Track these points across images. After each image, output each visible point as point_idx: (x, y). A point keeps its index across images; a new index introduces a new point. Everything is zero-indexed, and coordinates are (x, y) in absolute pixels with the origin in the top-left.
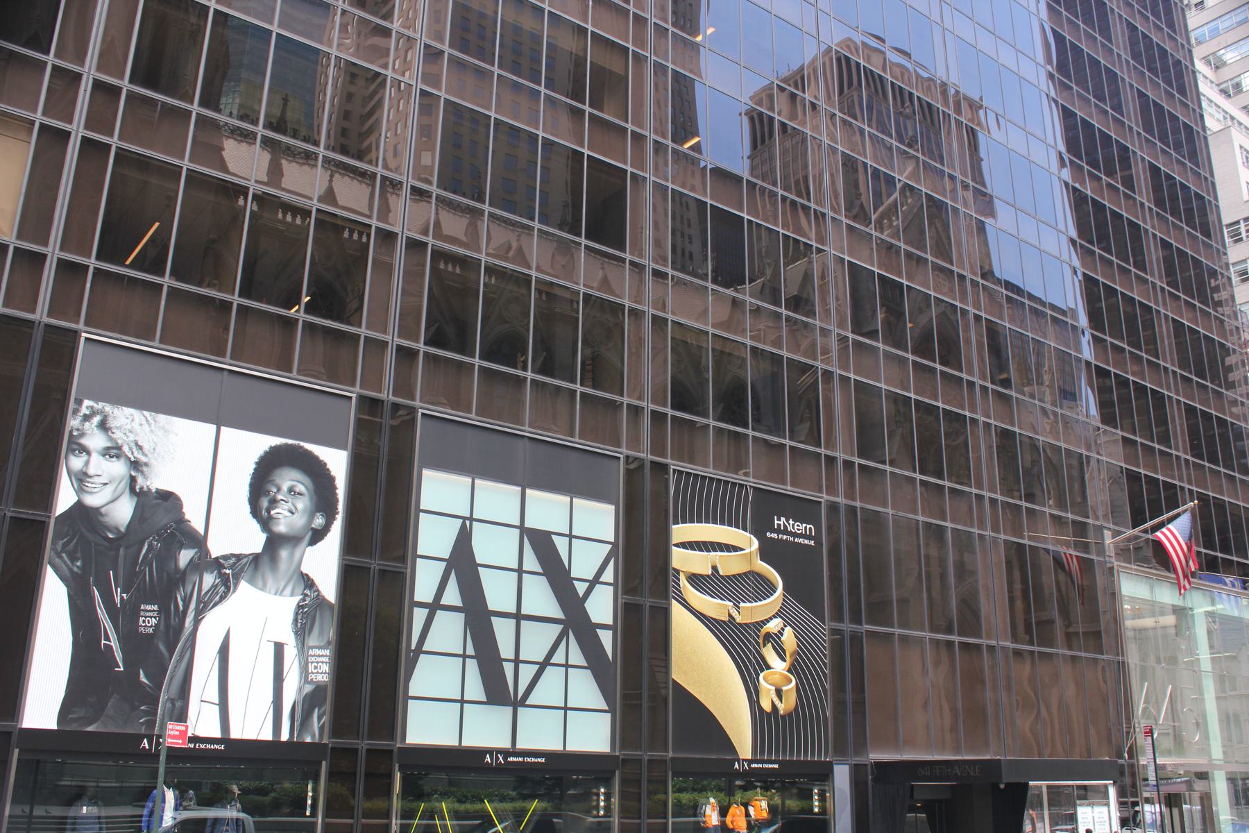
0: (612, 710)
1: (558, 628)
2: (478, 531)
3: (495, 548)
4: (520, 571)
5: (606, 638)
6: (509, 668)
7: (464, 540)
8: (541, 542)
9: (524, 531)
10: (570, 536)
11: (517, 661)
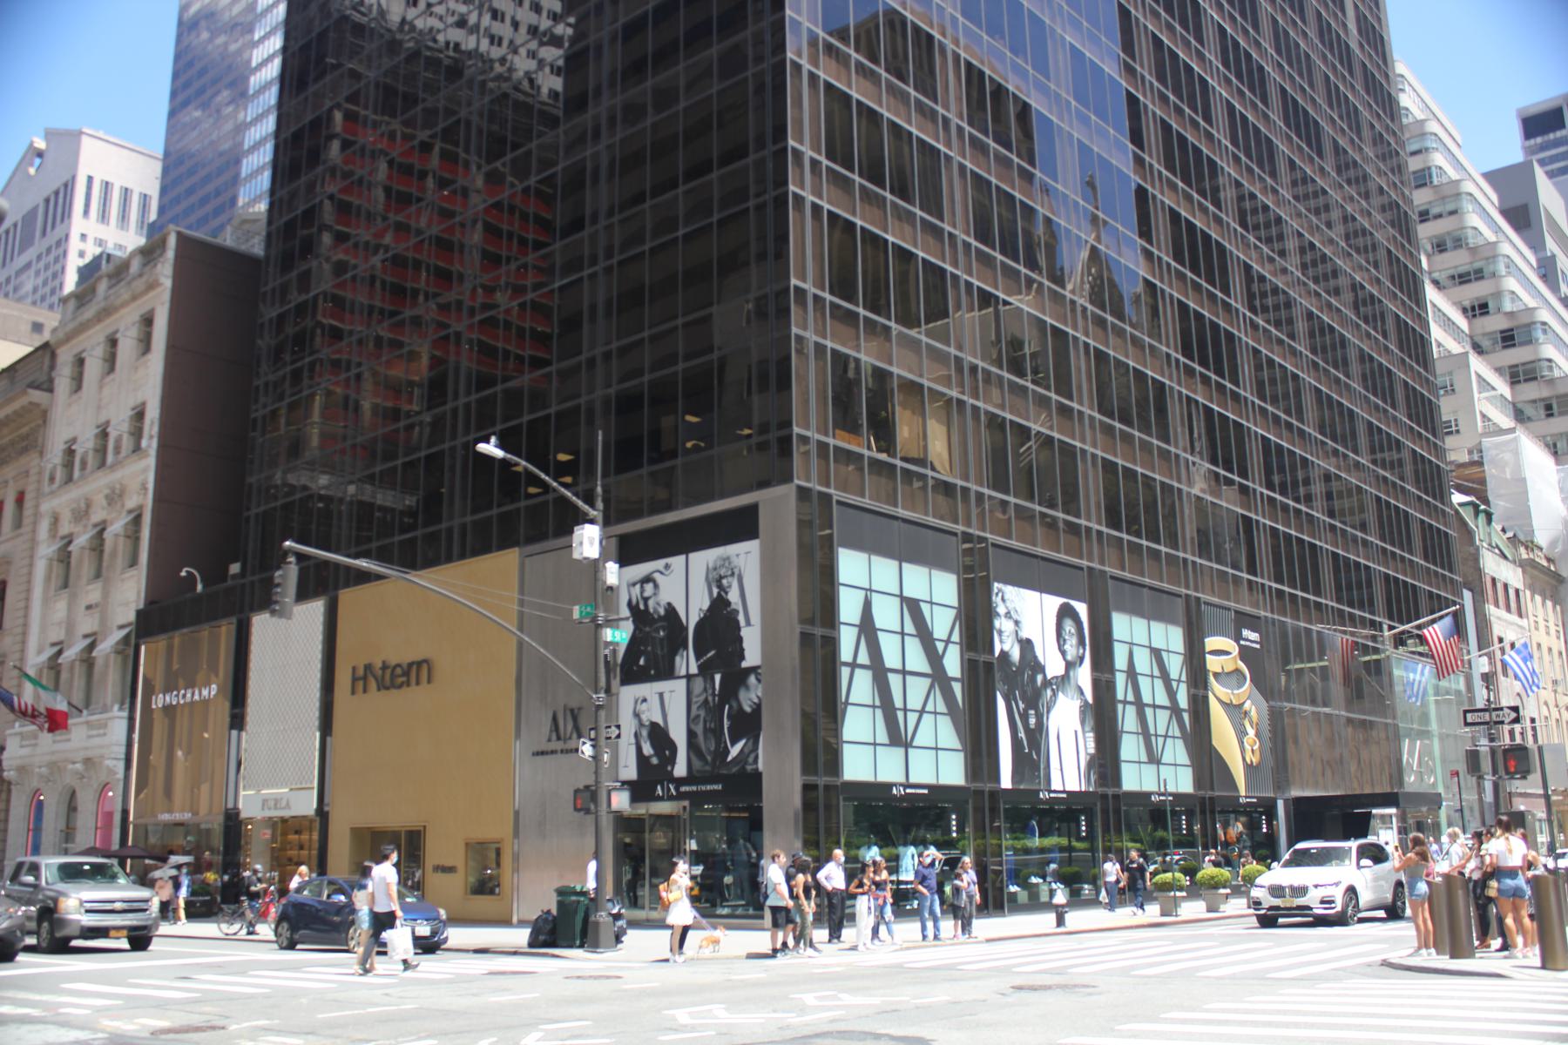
0: (964, 750)
1: (928, 681)
2: (875, 598)
3: (887, 615)
4: (902, 634)
5: (957, 688)
6: (900, 715)
7: (867, 605)
8: (912, 607)
9: (901, 596)
10: (931, 603)
11: (905, 710)
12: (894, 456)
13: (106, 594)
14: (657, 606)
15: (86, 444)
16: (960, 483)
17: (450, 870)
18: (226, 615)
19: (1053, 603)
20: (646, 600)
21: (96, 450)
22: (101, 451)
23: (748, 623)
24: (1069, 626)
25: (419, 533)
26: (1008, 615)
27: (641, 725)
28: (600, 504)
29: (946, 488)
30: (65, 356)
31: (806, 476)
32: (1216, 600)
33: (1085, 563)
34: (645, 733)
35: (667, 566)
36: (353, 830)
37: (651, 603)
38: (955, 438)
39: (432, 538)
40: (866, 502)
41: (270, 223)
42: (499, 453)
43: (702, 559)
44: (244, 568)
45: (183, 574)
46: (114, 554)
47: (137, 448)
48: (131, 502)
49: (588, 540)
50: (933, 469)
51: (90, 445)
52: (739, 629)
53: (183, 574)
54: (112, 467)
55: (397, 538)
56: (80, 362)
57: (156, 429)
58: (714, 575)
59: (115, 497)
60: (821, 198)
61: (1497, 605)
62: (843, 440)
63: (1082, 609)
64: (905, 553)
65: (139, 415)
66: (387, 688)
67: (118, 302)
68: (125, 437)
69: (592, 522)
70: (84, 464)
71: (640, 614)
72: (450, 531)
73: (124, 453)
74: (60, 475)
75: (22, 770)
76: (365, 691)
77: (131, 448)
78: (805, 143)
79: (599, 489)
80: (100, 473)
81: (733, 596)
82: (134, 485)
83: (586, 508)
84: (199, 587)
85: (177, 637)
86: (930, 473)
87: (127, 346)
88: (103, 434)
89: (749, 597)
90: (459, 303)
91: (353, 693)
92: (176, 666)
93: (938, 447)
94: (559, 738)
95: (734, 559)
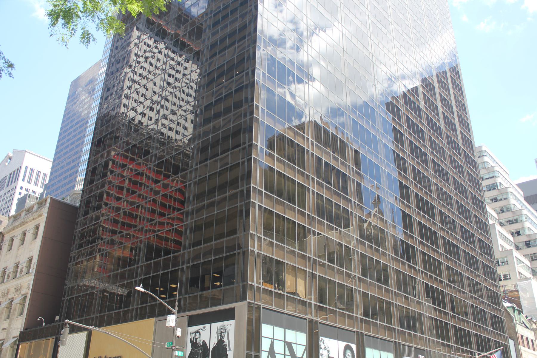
3: (279, 348)
4: (285, 355)
7: (272, 345)
8: (289, 345)
9: (285, 341)
10: (296, 344)
12: (284, 292)
13: (10, 325)
14: (200, 342)
15: (11, 269)
16: (308, 301)
18: (51, 336)
19: (343, 344)
20: (196, 339)
21: (14, 272)
22: (15, 272)
23: (230, 350)
24: (348, 352)
25: (122, 310)
26: (325, 348)
28: (177, 308)
29: (303, 303)
30: (7, 238)
31: (253, 298)
32: (407, 344)
33: (355, 330)
35: (204, 327)
37: (198, 340)
38: (307, 285)
39: (126, 312)
40: (274, 308)
41: (82, 197)
42: (143, 290)
43: (216, 326)
44: (60, 318)
46: (15, 309)
47: (28, 273)
48: (23, 292)
49: (171, 320)
50: (299, 296)
51: (12, 270)
52: (227, 351)
55: (114, 312)
56: (12, 240)
57: (35, 266)
58: (219, 331)
59: (18, 289)
60: (262, 203)
61: (524, 346)
62: (266, 286)
63: (354, 346)
64: (286, 326)
65: (30, 260)
67: (28, 220)
68: (24, 268)
69: (173, 314)
70: (8, 276)
71: (194, 344)
72: (133, 309)
73: (23, 274)
77: (26, 272)
78: (257, 184)
79: (177, 303)
80: (14, 280)
81: (225, 340)
82: (25, 285)
83: (172, 309)
84: (44, 324)
85: (34, 343)
86: (297, 298)
87: (29, 236)
88: (17, 266)
89: (230, 340)
90: (142, 228)
92: (31, 354)
93: (301, 288)
95: (226, 326)
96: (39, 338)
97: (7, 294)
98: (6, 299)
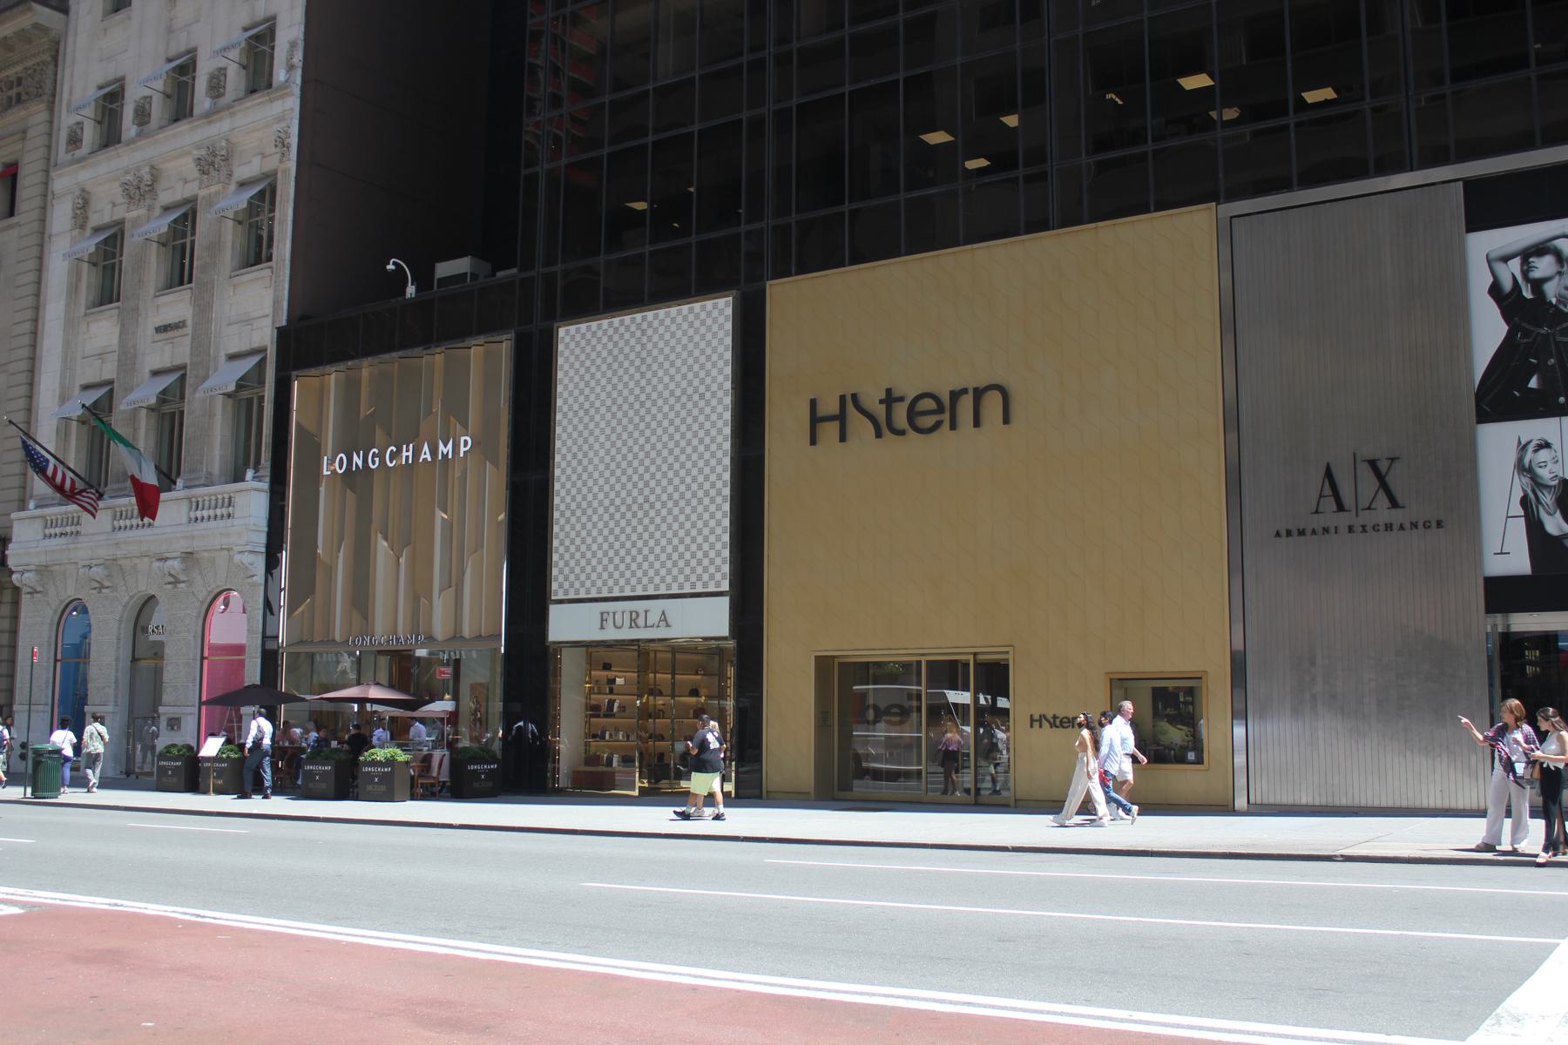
13: (203, 309)
15: (146, 82)
17: (1036, 721)
27: (1537, 483)
34: (1548, 498)
36: (824, 665)
45: (391, 267)
46: (215, 247)
53: (391, 267)
54: (208, 115)
57: (298, 58)
66: (902, 433)
70: (142, 115)
74: (89, 135)
75: (43, 570)
76: (953, 426)
84: (411, 290)
85: (367, 369)
91: (813, 442)
92: (365, 410)
94: (1341, 507)
96: (402, 347)
97: (152, 188)
98: (150, 208)
